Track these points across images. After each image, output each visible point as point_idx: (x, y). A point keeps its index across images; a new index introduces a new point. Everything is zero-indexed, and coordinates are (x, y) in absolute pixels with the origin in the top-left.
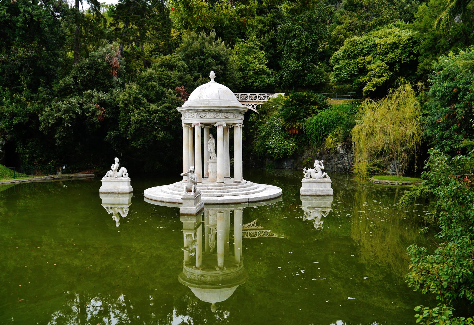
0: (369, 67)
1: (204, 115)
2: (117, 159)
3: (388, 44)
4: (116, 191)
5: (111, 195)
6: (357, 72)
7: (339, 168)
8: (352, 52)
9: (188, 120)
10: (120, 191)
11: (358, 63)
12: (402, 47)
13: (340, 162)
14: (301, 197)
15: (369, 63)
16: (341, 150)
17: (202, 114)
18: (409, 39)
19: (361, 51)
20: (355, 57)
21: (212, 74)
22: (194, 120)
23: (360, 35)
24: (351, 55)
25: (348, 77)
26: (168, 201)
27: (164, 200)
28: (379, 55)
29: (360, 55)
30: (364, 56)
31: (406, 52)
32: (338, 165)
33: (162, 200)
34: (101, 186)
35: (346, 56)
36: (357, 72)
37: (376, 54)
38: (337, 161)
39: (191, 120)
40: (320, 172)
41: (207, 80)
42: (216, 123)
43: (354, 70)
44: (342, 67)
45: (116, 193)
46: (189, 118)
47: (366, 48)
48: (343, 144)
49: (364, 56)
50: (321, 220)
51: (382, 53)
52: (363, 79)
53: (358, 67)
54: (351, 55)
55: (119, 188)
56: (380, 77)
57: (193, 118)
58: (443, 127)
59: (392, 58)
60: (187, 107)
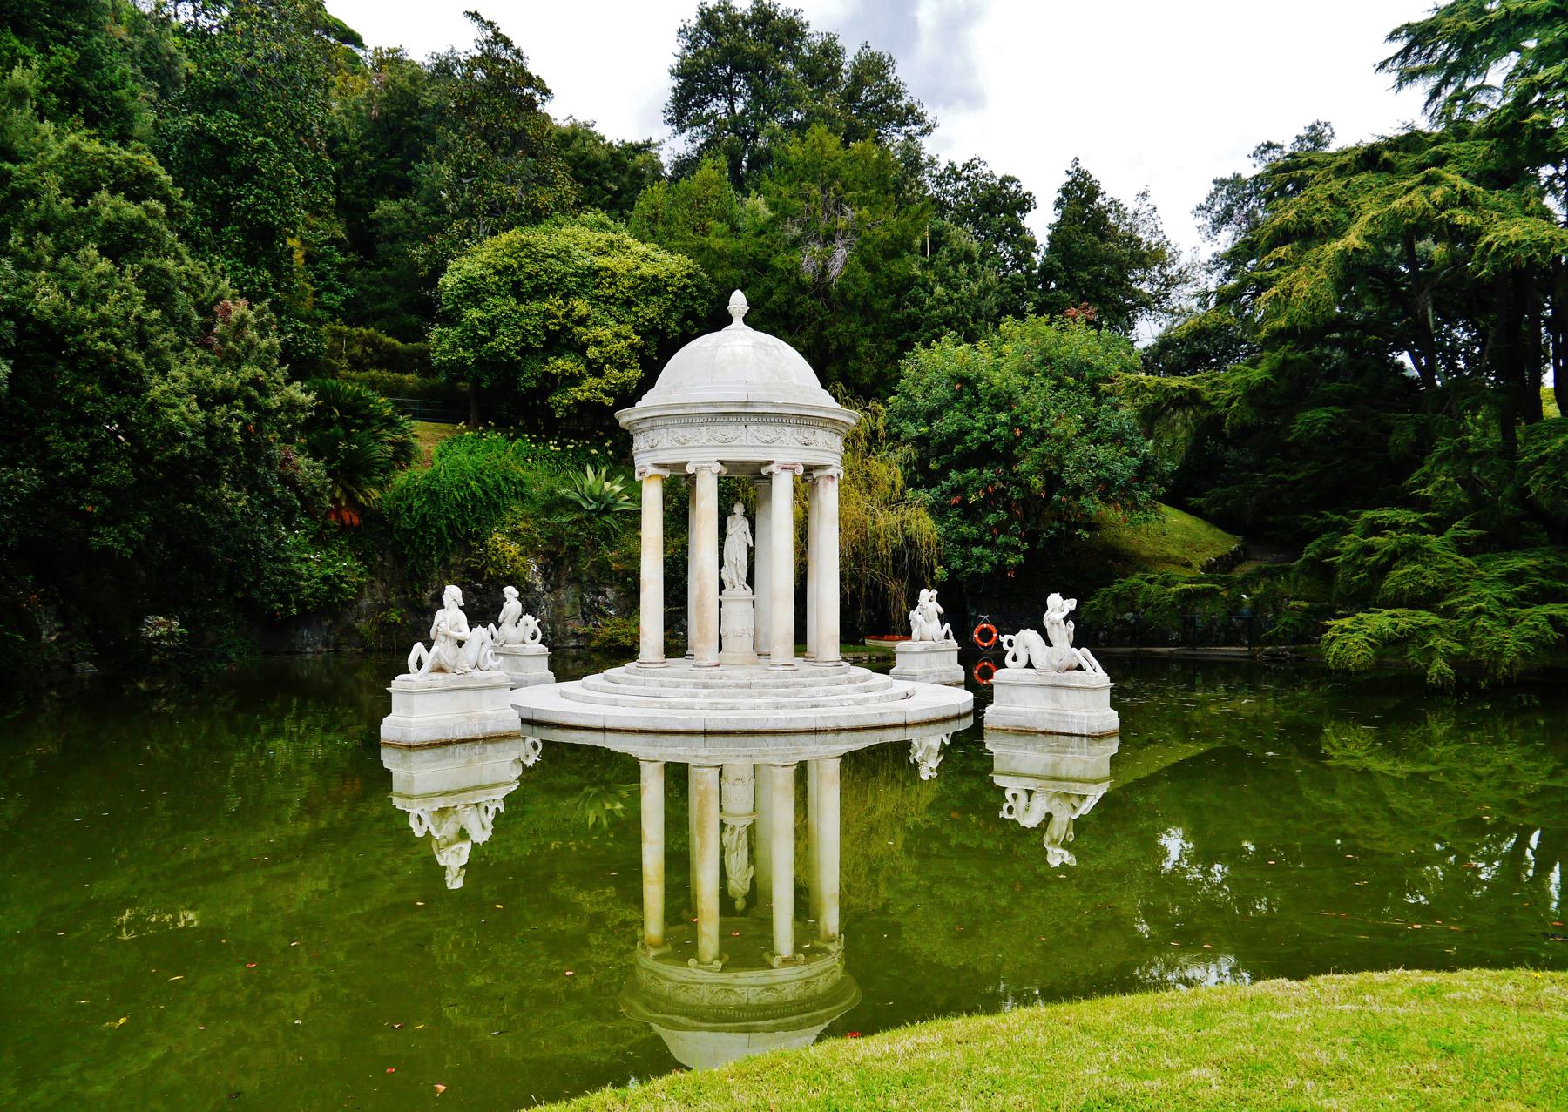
0: (583, 333)
1: (811, 438)
2: (453, 594)
3: (642, 278)
4: (478, 732)
5: (459, 748)
6: (542, 342)
8: (529, 277)
9: (752, 450)
10: (490, 728)
11: (548, 315)
12: (673, 292)
14: (383, 752)
15: (582, 321)
16: (538, 580)
18: (689, 276)
19: (560, 280)
20: (539, 292)
21: (738, 302)
23: (703, 250)
24: (528, 285)
25: (518, 353)
26: (844, 725)
27: (830, 725)
28: (605, 302)
29: (552, 291)
30: (565, 297)
31: (676, 307)
33: (821, 725)
34: (389, 711)
35: (509, 286)
36: (542, 342)
37: (597, 298)
41: (720, 320)
43: (535, 334)
44: (499, 321)
45: (475, 740)
47: (572, 275)
48: (540, 561)
49: (565, 297)
50: (940, 753)
51: (618, 299)
52: (564, 364)
53: (545, 327)
54: (528, 285)
55: (486, 718)
56: (622, 367)
58: (959, 515)
59: (651, 320)
60: (774, 405)
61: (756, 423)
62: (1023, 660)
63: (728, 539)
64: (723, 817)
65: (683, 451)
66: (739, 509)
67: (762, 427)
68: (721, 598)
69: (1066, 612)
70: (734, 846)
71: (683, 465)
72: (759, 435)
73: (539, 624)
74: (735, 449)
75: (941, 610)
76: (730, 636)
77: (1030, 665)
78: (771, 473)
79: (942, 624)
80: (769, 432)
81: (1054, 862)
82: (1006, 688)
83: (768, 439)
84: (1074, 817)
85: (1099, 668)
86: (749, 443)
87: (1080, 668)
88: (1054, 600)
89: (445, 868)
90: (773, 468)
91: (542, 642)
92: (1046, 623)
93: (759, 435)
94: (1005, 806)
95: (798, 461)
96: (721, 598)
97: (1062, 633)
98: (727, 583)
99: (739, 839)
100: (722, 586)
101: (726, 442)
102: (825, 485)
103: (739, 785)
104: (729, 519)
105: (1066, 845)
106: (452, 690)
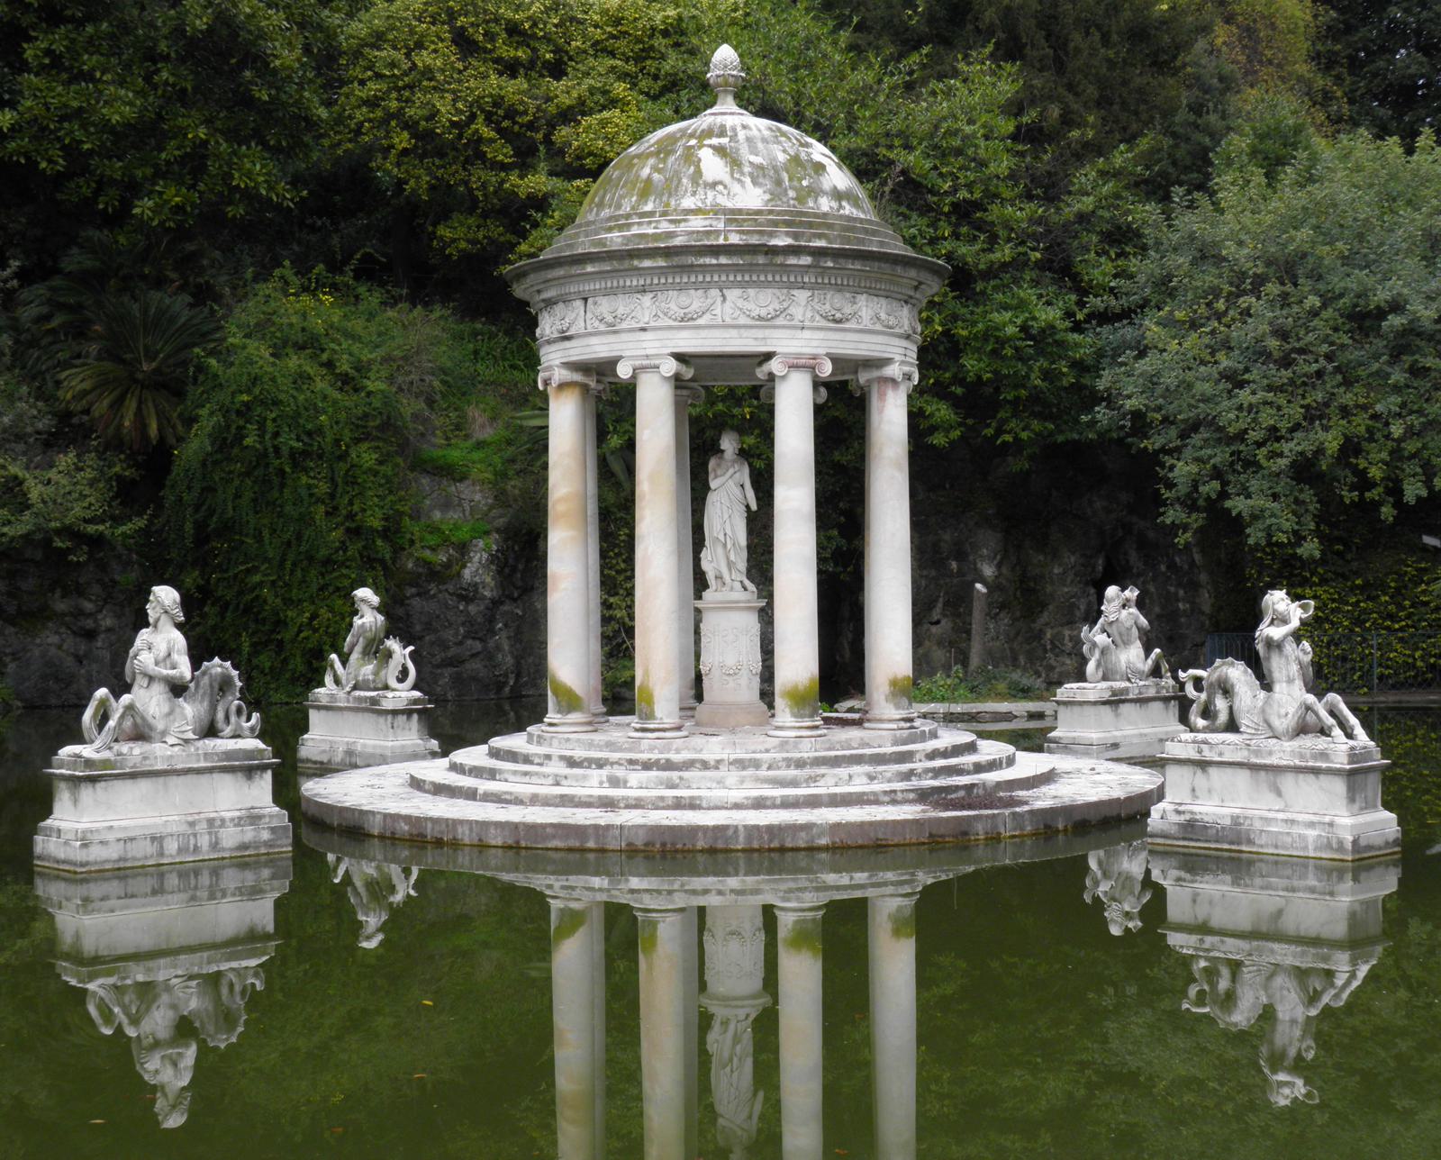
1: (848, 310)
7: (474, 679)
9: (734, 333)
13: (478, 646)
17: (684, 299)
22: (787, 333)
32: (468, 666)
38: (461, 643)
39: (760, 333)
46: (743, 320)
57: (780, 321)
61: (743, 285)
62: (1223, 717)
63: (712, 498)
64: (705, 1001)
65: (612, 338)
66: (728, 444)
67: (751, 292)
68: (699, 604)
69: (1295, 623)
70: (726, 1054)
71: (612, 363)
72: (751, 306)
73: (411, 654)
74: (704, 333)
75: (1143, 621)
76: (716, 673)
77: (1232, 726)
78: (772, 377)
79: (1148, 651)
80: (763, 300)
81: (1282, 1099)
82: (1186, 772)
83: (763, 313)
84: (1313, 1012)
85: (1359, 731)
86: (728, 321)
87: (1324, 731)
88: (1277, 599)
89: (154, 1088)
90: (775, 366)
91: (415, 687)
92: (1260, 647)
93: (751, 306)
94: (1193, 991)
95: (822, 351)
96: (699, 604)
97: (1291, 664)
98: (710, 577)
99: (736, 1040)
100: (700, 582)
101: (687, 321)
102: (882, 396)
103: (734, 945)
104: (712, 463)
105: (1299, 1066)
106: (199, 771)
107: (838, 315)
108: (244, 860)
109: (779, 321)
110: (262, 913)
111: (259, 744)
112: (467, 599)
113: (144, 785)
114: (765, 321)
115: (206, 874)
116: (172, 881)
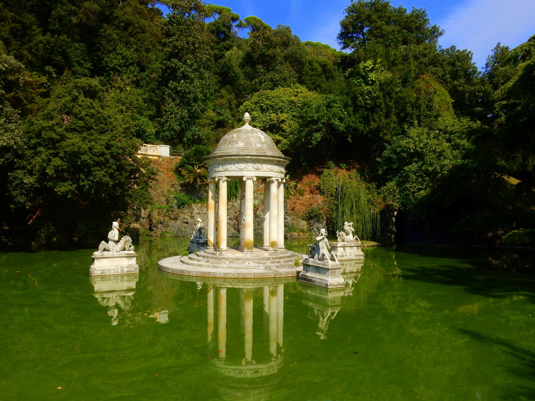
39: (241, 172)
40: (351, 236)
42: (271, 177)
46: (238, 169)
83: (242, 168)
101: (226, 170)
107: (258, 168)
108: (129, 275)
109: (245, 169)
110: (133, 285)
111: (134, 252)
112: (258, 218)
113: (107, 259)
114: (241, 170)
115: (120, 278)
116: (112, 278)
